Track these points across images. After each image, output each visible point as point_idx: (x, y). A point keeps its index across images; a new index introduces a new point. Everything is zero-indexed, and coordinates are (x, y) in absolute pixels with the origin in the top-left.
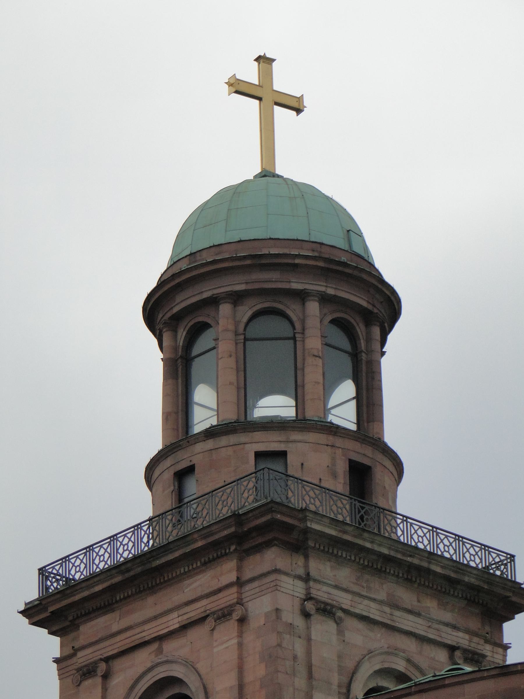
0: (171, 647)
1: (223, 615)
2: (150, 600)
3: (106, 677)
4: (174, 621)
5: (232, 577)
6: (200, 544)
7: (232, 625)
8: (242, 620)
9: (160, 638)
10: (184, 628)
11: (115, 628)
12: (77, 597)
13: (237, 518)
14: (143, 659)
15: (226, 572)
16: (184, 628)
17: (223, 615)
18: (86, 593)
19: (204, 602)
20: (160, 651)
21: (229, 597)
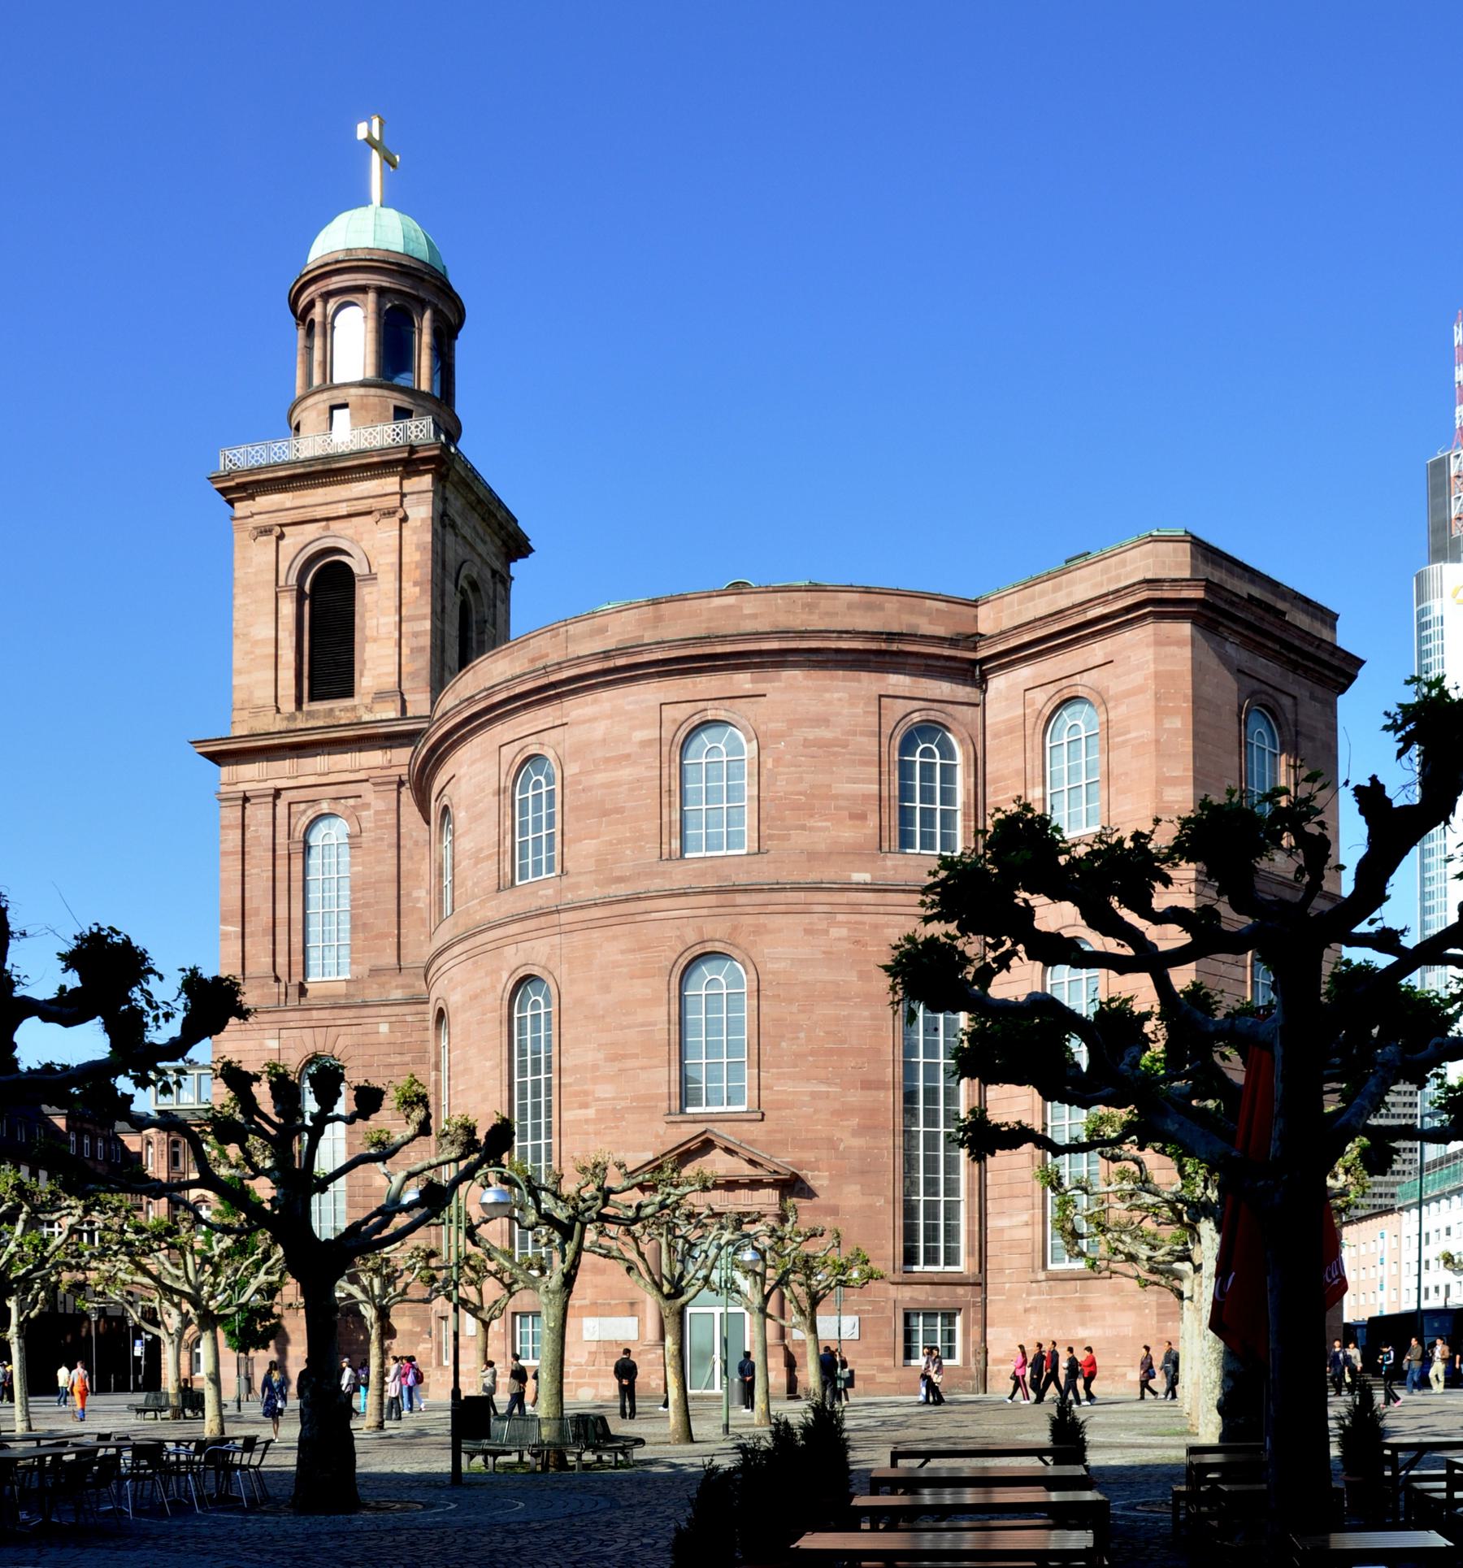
0: (335, 526)
1: (390, 513)
2: (321, 491)
3: (281, 537)
4: (343, 509)
5: (397, 488)
6: (375, 459)
8: (404, 519)
9: (328, 519)
10: (350, 516)
11: (288, 505)
12: (262, 477)
13: (412, 449)
14: (311, 531)
15: (391, 483)
16: (350, 516)
17: (390, 513)
18: (270, 475)
20: (327, 528)
21: (394, 501)
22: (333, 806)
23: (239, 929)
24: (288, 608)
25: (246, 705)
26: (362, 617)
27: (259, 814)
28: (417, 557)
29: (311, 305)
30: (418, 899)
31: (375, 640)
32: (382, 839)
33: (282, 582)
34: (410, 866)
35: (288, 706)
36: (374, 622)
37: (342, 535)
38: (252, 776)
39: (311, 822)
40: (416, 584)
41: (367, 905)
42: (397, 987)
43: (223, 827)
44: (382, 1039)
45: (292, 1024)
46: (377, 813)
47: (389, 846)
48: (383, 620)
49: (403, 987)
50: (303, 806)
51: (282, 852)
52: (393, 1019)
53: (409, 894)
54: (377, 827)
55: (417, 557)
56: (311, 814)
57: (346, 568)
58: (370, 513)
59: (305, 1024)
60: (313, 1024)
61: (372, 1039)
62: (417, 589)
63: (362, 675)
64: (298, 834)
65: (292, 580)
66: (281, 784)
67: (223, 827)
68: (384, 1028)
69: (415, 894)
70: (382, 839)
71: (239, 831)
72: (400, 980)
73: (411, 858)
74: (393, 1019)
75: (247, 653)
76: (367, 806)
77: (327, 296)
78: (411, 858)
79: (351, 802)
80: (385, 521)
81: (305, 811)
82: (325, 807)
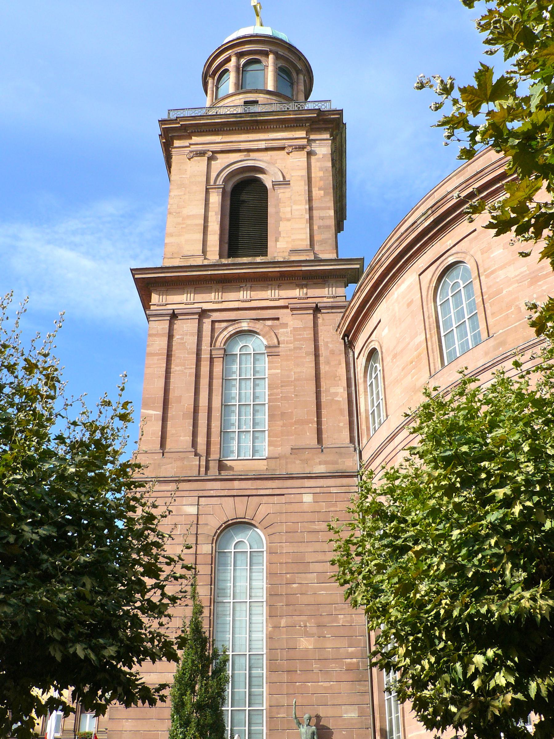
4: (262, 145)
5: (305, 136)
7: (304, 154)
10: (267, 149)
16: (267, 149)
19: (285, 141)
21: (305, 142)
22: (252, 324)
23: (160, 413)
24: (215, 199)
25: (175, 256)
26: (277, 206)
27: (186, 329)
28: (321, 174)
29: (228, 60)
30: (336, 394)
31: (289, 220)
32: (301, 348)
33: (212, 182)
34: (327, 368)
35: (213, 256)
36: (289, 209)
37: (260, 160)
38: (178, 300)
39: (231, 336)
40: (320, 189)
41: (285, 398)
42: (320, 463)
43: (150, 335)
44: (305, 508)
45: (212, 493)
46: (295, 329)
47: (307, 354)
48: (295, 207)
49: (326, 463)
50: (224, 325)
51: (205, 356)
52: (318, 490)
53: (327, 390)
54: (296, 340)
55: (321, 174)
56: (232, 329)
57: (259, 181)
58: (283, 148)
59: (225, 493)
60: (234, 493)
61: (295, 507)
62: (322, 192)
63: (277, 240)
64: (220, 343)
65: (220, 181)
66: (206, 306)
67: (150, 335)
68: (308, 498)
69: (332, 390)
70: (301, 348)
71: (166, 339)
72: (323, 457)
73: (328, 363)
74: (318, 490)
75: (179, 224)
76: (285, 325)
77: (240, 55)
78: (328, 363)
79: (269, 323)
80: (296, 154)
81: (226, 328)
82: (244, 326)
